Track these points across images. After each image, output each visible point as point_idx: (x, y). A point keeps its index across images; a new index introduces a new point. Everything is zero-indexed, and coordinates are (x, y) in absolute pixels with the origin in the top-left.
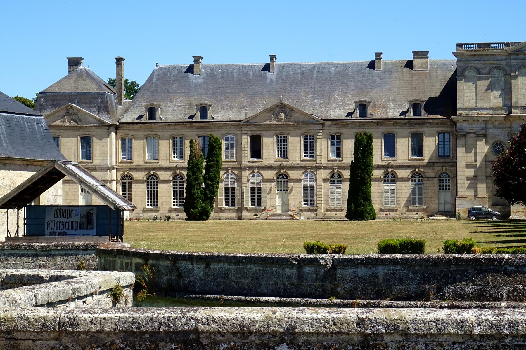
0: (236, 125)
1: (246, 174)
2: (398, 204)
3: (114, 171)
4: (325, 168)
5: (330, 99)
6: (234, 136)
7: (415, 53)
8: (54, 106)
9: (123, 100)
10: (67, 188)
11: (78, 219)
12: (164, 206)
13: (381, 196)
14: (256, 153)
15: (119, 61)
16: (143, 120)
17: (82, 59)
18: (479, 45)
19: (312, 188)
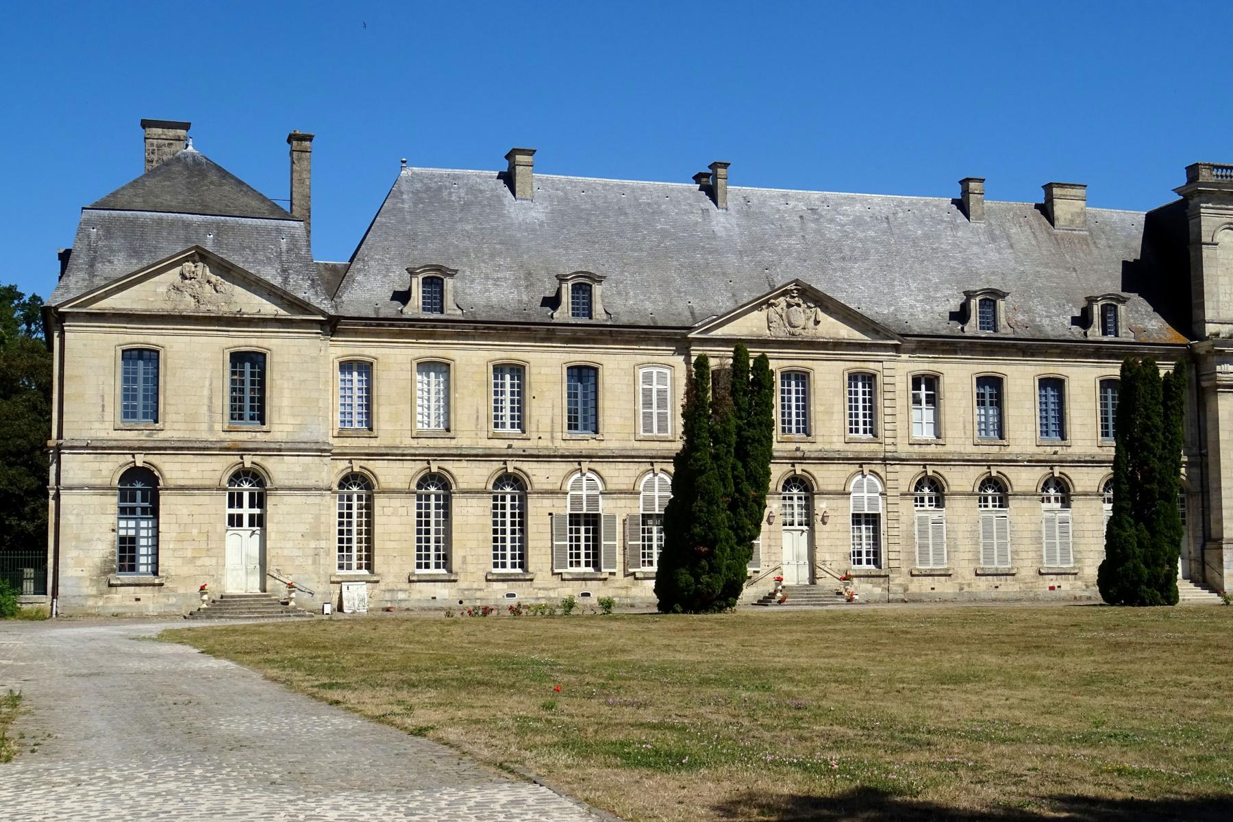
2: (1077, 560)
4: (902, 461)
6: (668, 371)
10: (185, 511)
12: (471, 568)
13: (1038, 540)
19: (873, 520)
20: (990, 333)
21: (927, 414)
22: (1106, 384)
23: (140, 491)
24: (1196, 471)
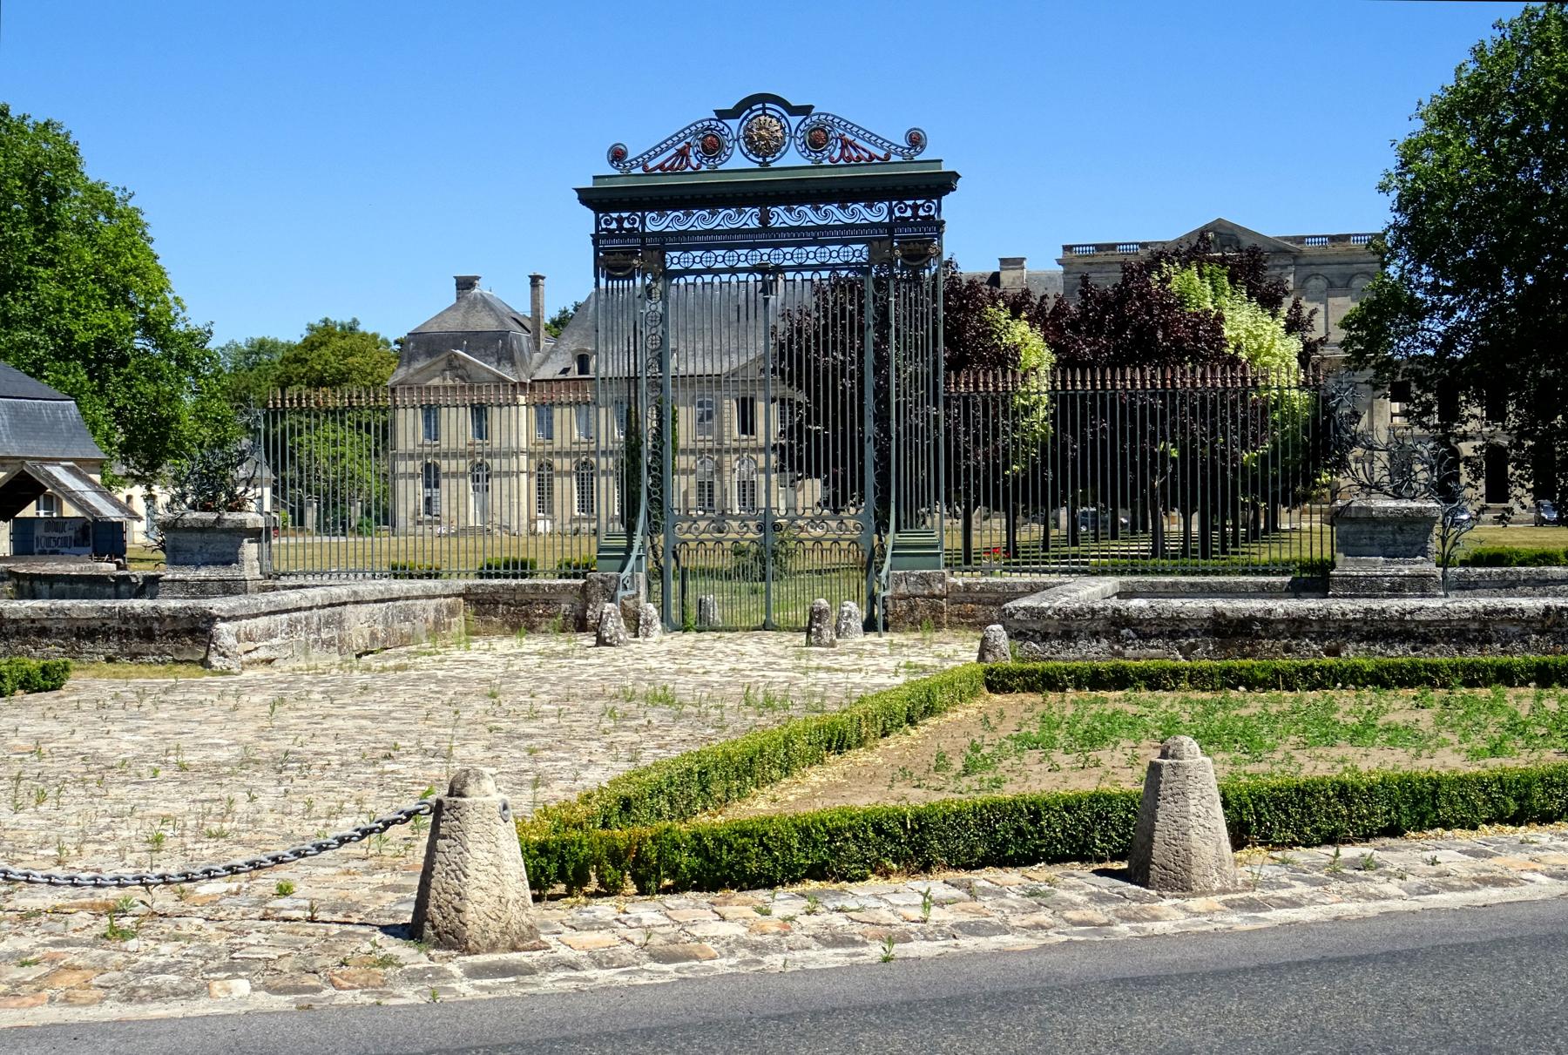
0: (715, 381)
1: (730, 461)
3: (524, 458)
7: (1003, 261)
8: (430, 354)
9: (543, 344)
11: (71, 533)
14: (747, 426)
15: (535, 280)
16: (570, 375)
17: (478, 278)
18: (1099, 247)
23: (432, 476)
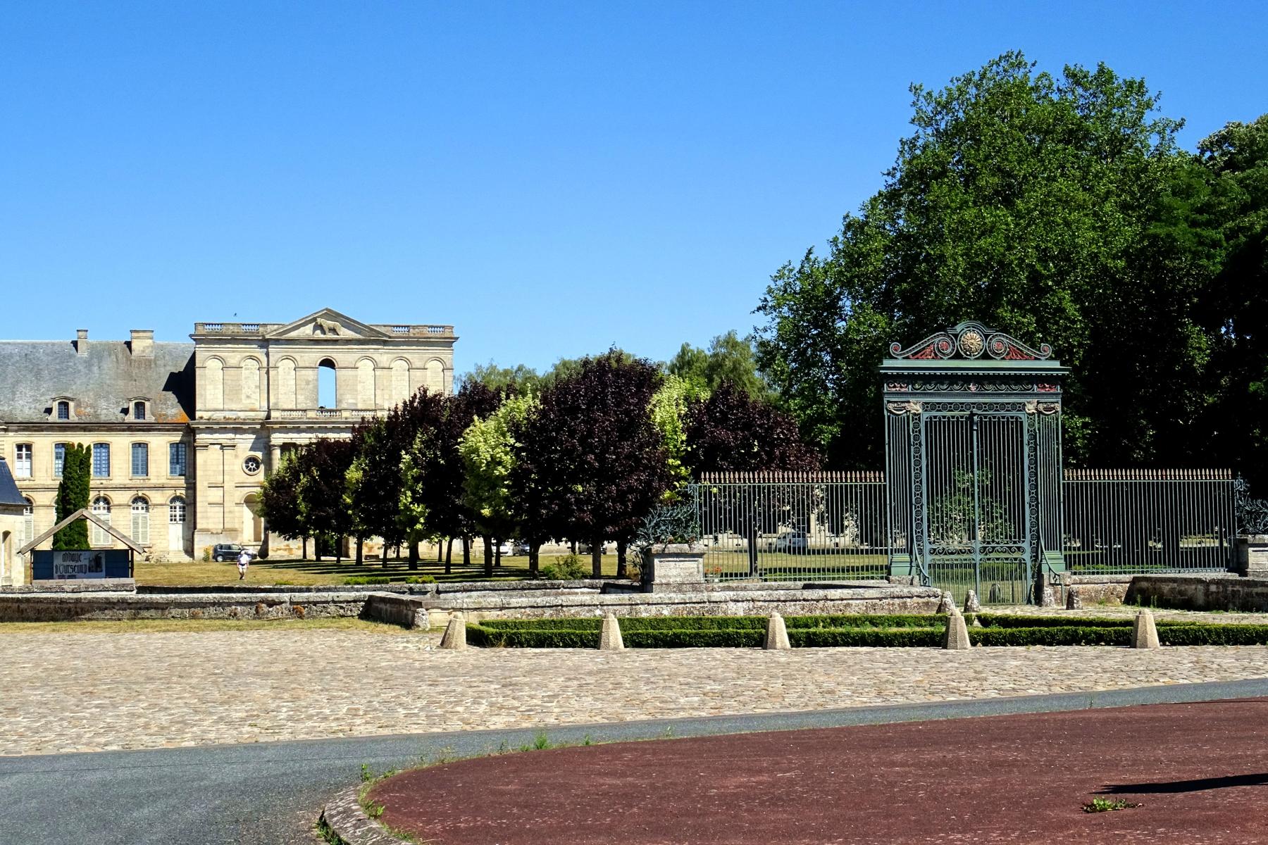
5: (14, 393)
20: (65, 420)
21: (28, 464)
22: (172, 445)
24: (191, 492)
